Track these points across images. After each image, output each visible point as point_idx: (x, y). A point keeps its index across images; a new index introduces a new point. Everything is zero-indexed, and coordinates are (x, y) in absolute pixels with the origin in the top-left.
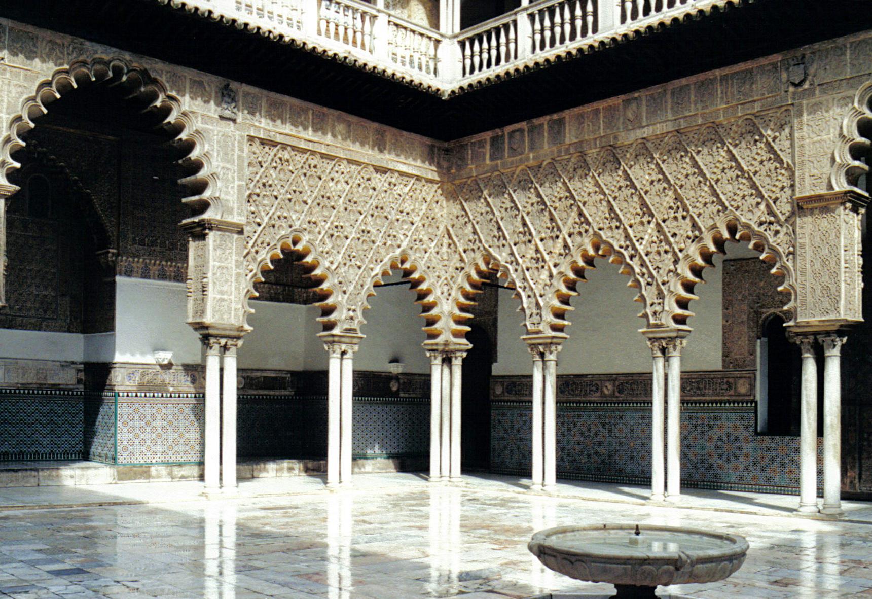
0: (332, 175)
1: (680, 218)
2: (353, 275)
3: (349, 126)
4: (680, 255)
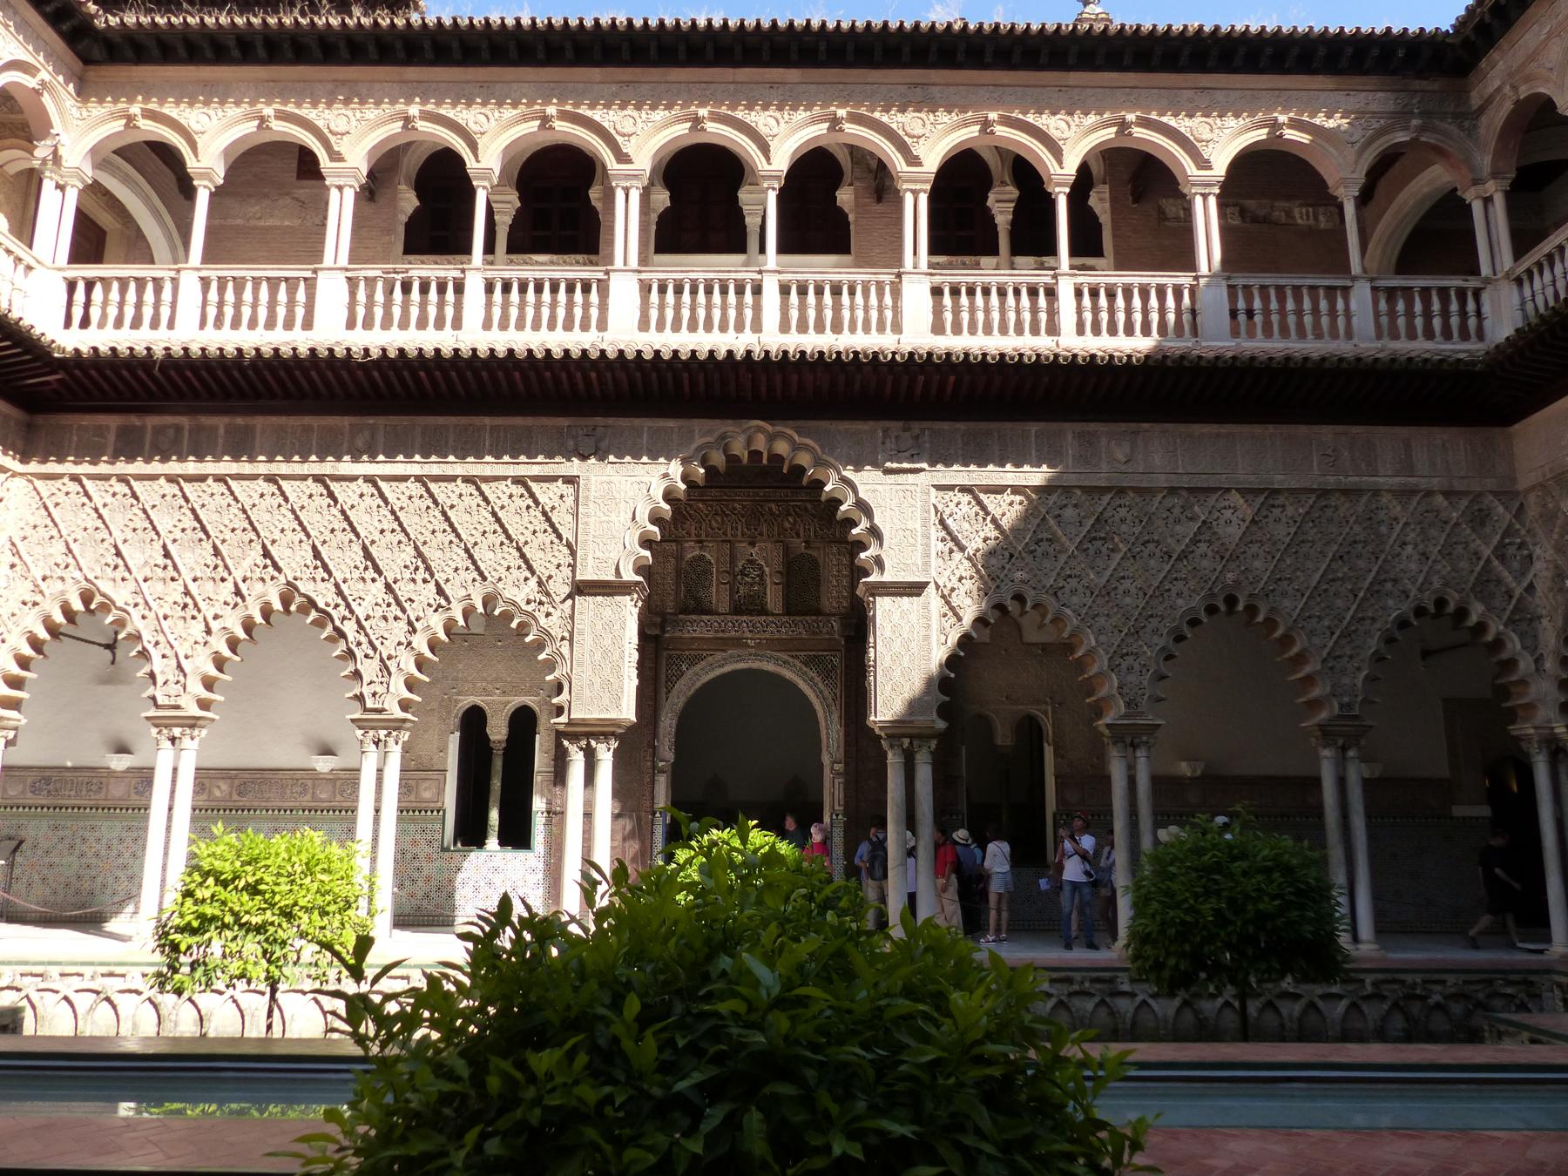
1: (419, 581)
4: (418, 625)
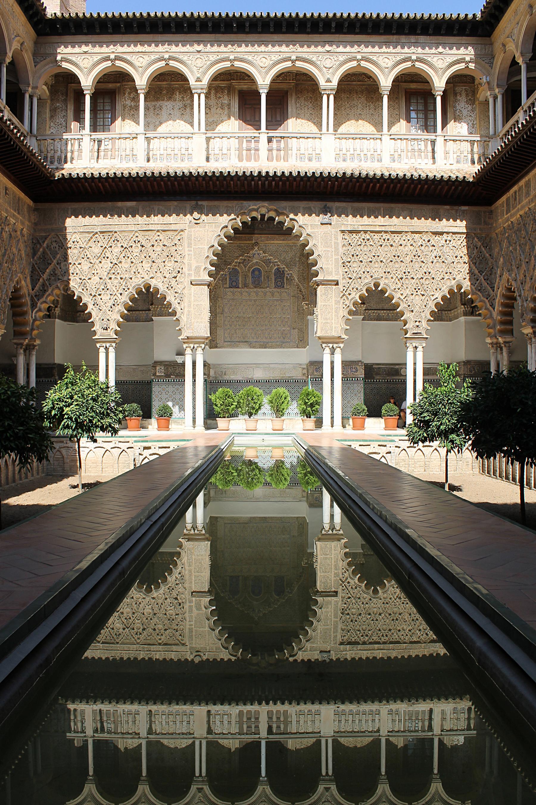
0: (400, 243)
2: (417, 300)
3: (411, 211)
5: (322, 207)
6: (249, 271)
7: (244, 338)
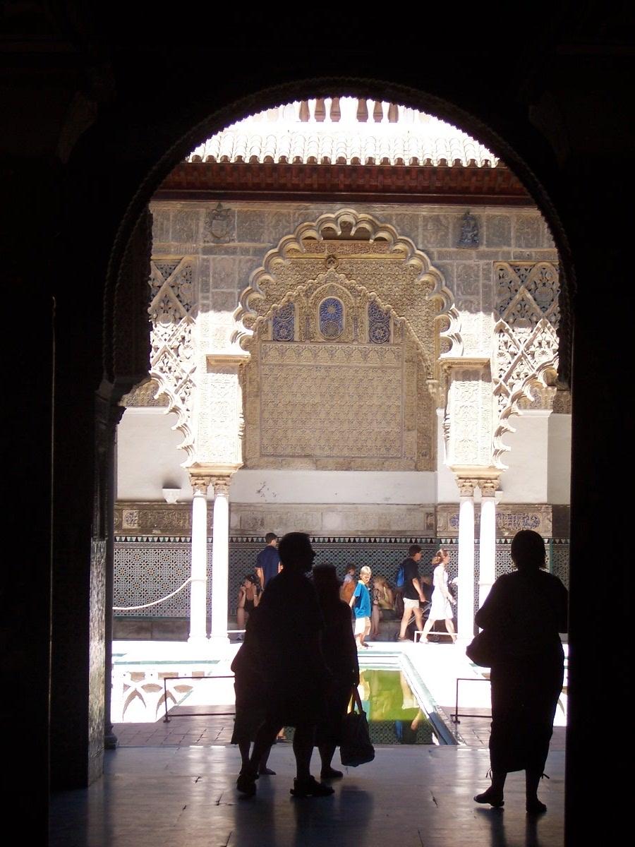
5: (460, 216)
6: (315, 304)
7: (303, 449)
